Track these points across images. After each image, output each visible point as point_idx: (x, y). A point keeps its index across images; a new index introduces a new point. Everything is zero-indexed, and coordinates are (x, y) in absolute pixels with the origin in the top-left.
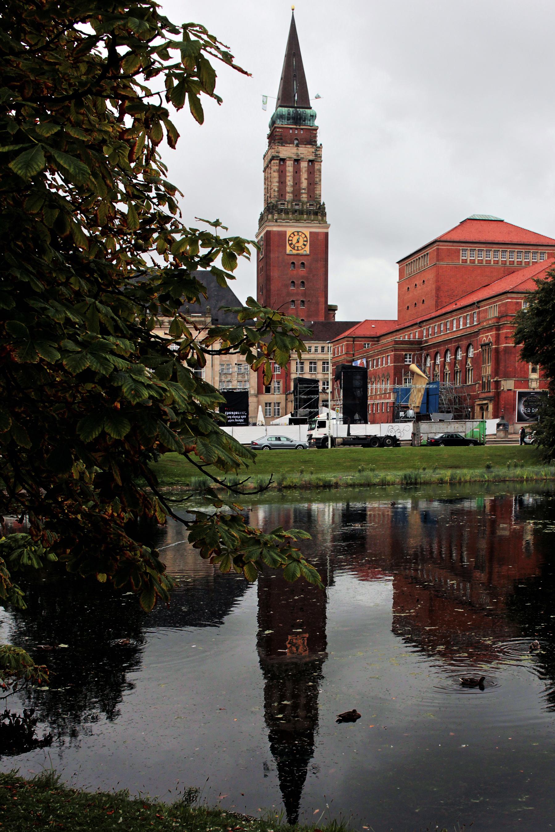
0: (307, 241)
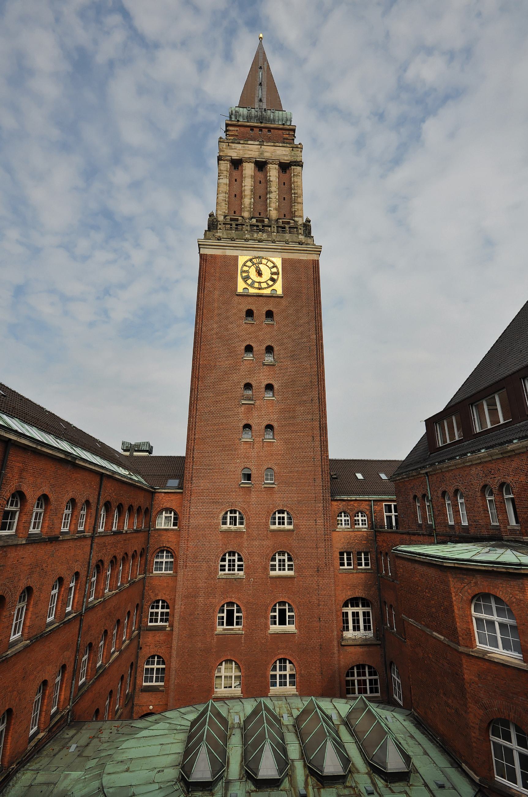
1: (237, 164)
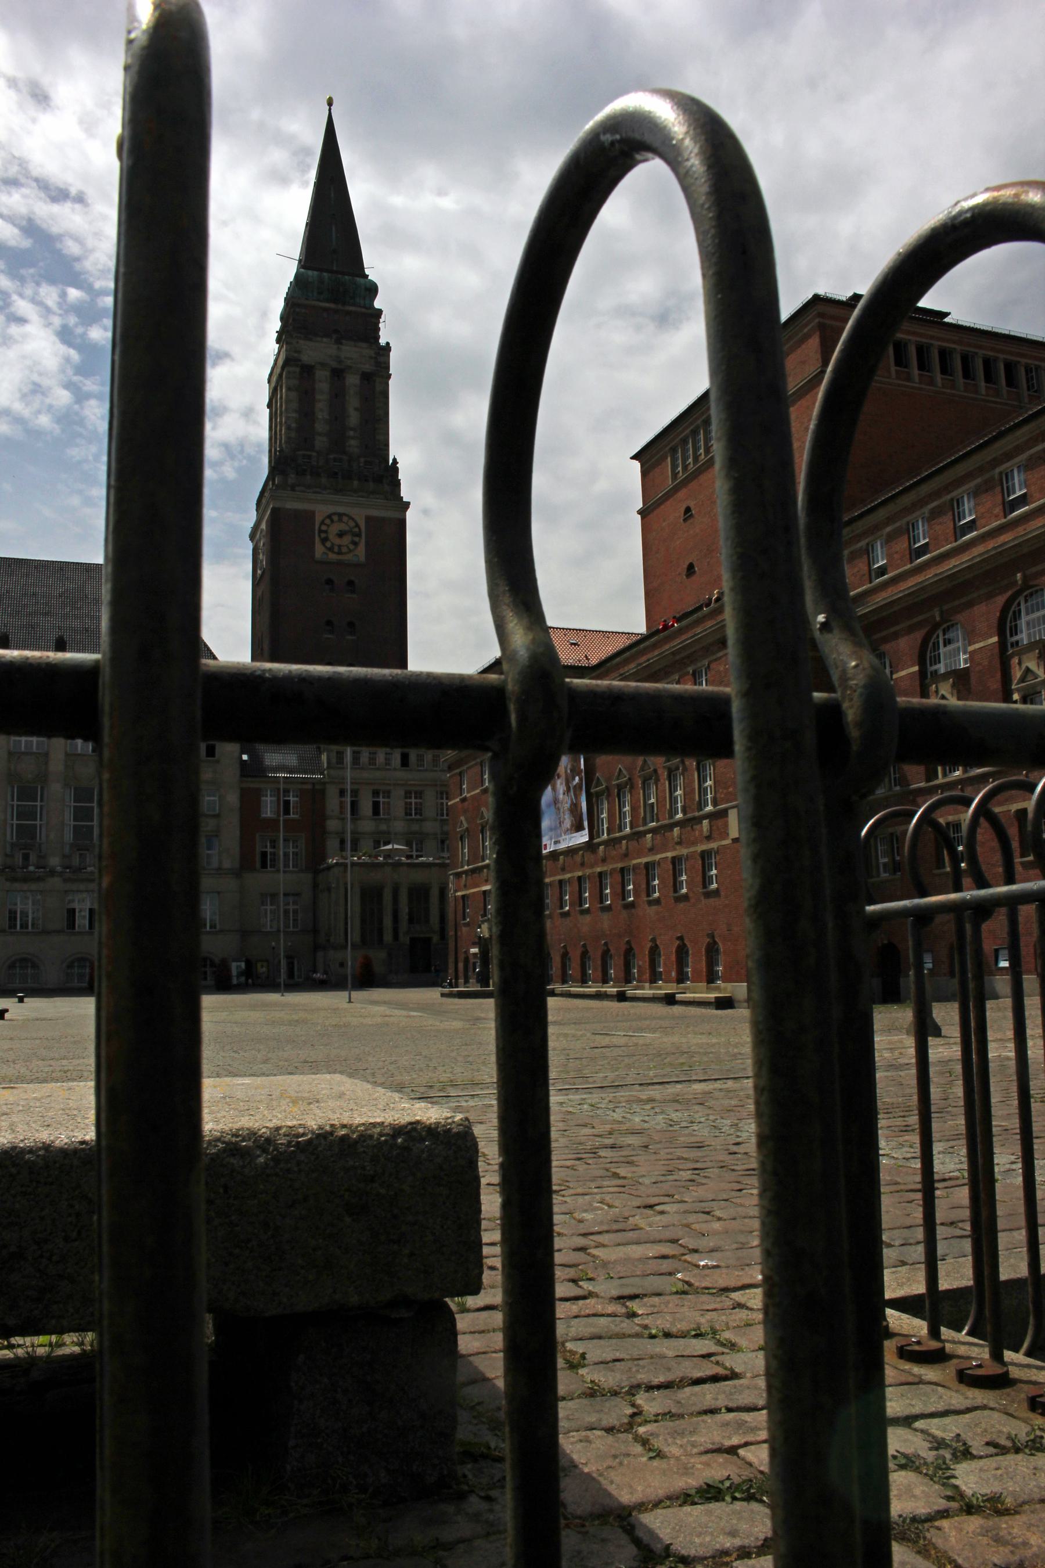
0: (359, 535)
1: (307, 371)
